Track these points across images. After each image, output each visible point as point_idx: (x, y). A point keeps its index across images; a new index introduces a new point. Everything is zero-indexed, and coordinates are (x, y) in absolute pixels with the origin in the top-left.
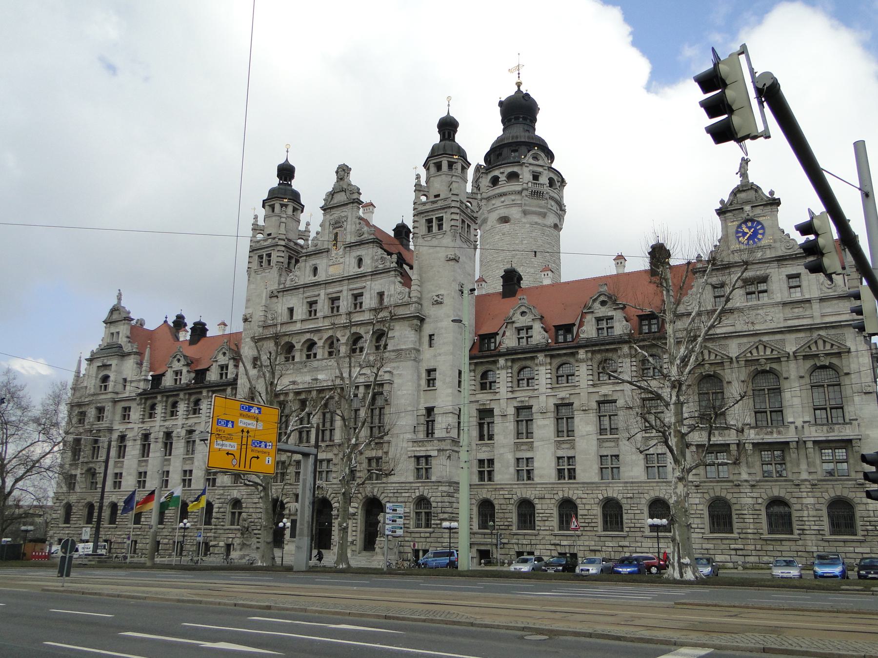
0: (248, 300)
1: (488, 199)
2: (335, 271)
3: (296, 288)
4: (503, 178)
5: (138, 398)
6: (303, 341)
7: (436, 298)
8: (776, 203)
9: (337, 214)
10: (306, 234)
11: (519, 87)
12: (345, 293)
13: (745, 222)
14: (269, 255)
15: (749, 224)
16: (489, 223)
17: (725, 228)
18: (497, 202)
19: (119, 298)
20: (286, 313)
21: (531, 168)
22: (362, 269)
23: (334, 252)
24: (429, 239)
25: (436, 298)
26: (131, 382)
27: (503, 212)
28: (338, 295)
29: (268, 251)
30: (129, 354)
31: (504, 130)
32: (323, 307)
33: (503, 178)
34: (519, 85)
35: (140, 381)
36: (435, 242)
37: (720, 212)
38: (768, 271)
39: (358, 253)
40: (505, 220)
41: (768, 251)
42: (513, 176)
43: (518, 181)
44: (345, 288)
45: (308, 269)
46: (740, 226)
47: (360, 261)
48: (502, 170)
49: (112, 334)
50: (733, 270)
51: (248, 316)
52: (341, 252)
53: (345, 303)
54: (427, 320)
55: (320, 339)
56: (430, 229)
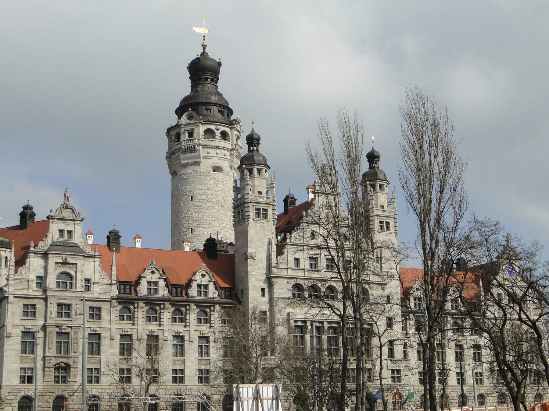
1: (205, 147)
4: (218, 133)
11: (204, 48)
14: (265, 210)
18: (212, 152)
20: (293, 261)
24: (383, 234)
27: (219, 163)
29: (265, 207)
33: (218, 133)
34: (204, 47)
40: (217, 169)
42: (224, 135)
48: (218, 127)
51: (253, 255)
56: (382, 228)
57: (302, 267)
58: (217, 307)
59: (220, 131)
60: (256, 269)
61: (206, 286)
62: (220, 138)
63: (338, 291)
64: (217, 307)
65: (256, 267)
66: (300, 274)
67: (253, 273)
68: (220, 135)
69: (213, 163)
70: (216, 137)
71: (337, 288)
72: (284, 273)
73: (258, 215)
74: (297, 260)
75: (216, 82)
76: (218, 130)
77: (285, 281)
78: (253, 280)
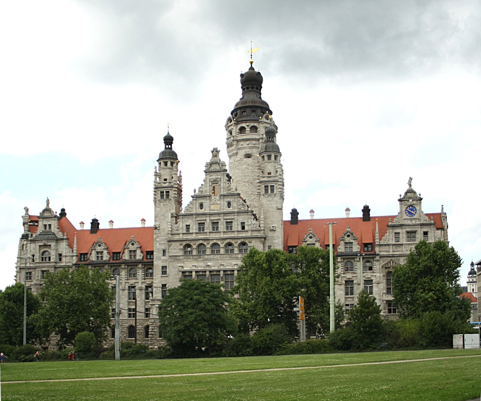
0: (156, 217)
1: (238, 141)
2: (215, 208)
3: (192, 215)
4: (248, 129)
5: (74, 267)
6: (197, 244)
7: (272, 228)
8: (421, 199)
9: (214, 176)
10: (180, 178)
12: (222, 220)
13: (409, 206)
15: (411, 207)
16: (238, 156)
17: (401, 208)
19: (48, 204)
21: (264, 125)
22: (231, 208)
23: (213, 198)
24: (267, 196)
25: (272, 228)
26: (66, 256)
27: (249, 151)
28: (217, 221)
30: (62, 239)
31: (242, 94)
32: (208, 227)
33: (248, 129)
35: (73, 256)
36: (270, 198)
37: (400, 200)
38: (416, 229)
39: (229, 200)
41: (417, 220)
42: (254, 129)
43: (256, 132)
44: (222, 218)
45: (197, 204)
46: (407, 208)
47: (229, 204)
48: (248, 124)
49: (45, 226)
50: (403, 227)
51: (157, 226)
52: (218, 197)
53: (222, 226)
54: (267, 238)
55: (208, 244)
56: (266, 191)
57: (191, 231)
58: (140, 265)
59: (250, 127)
60: (159, 237)
61: (102, 252)
62: (249, 132)
63: (221, 246)
64: (140, 265)
65: (159, 235)
66: (189, 237)
67: (157, 240)
68: (249, 130)
69: (246, 152)
70: (246, 132)
71: (220, 244)
72: (176, 237)
73: (162, 196)
74: (188, 226)
75: (260, 90)
76: (248, 126)
77: (178, 244)
78: (158, 244)
